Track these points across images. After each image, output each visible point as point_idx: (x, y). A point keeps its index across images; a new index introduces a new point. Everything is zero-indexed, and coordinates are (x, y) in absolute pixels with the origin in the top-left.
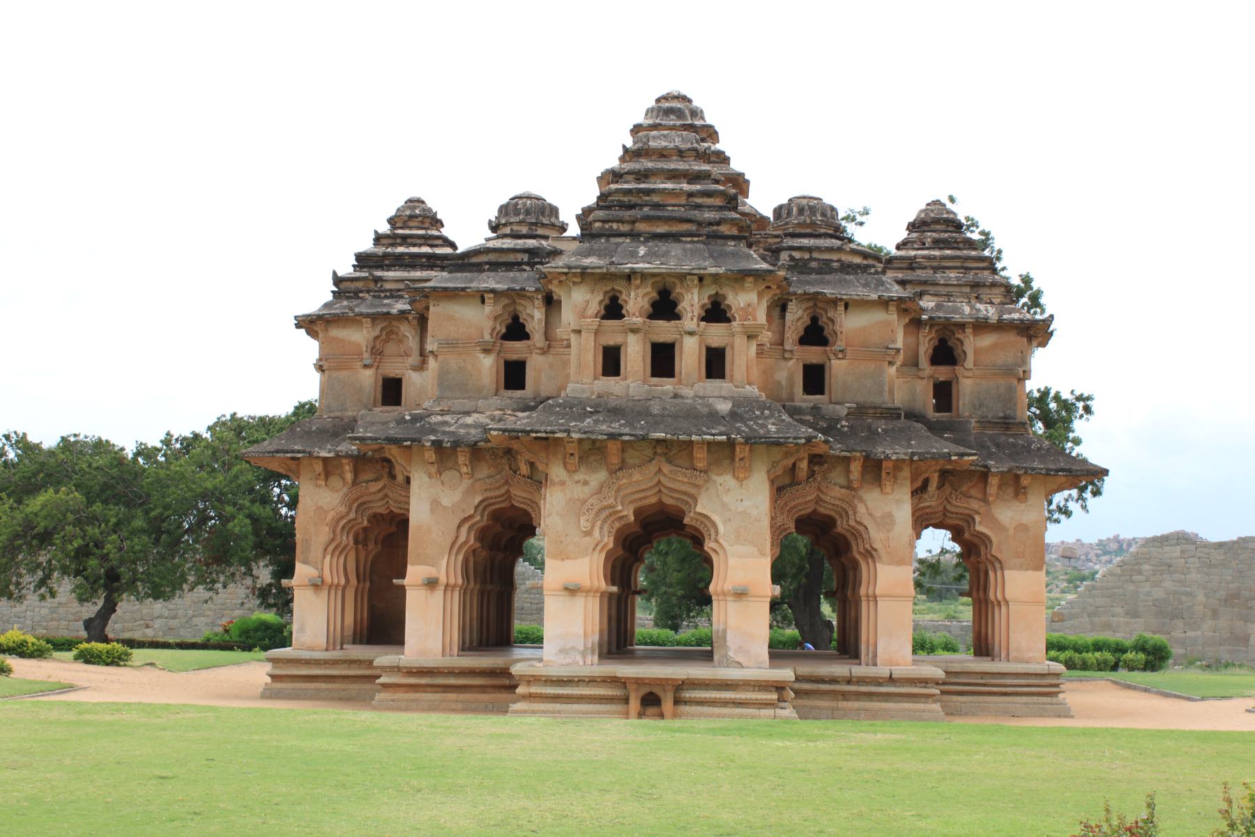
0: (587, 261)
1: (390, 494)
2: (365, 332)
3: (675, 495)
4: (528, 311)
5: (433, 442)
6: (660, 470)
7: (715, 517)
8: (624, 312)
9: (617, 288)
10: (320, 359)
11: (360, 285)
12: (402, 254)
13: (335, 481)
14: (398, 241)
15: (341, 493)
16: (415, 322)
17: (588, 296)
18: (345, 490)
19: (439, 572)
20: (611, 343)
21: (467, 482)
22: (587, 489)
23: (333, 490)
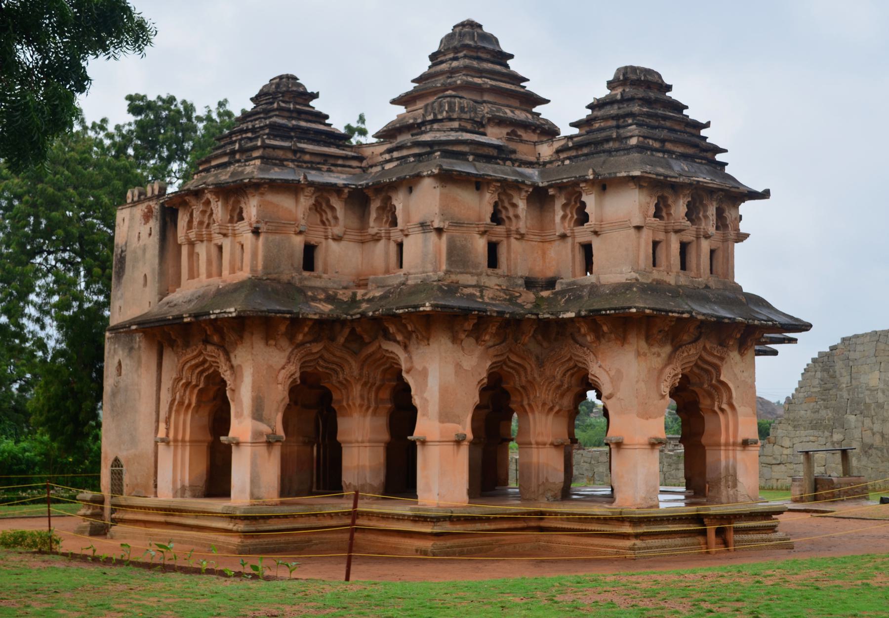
0: (661, 170)
1: (326, 355)
2: (302, 199)
3: (705, 366)
4: (515, 201)
5: (498, 312)
6: (705, 348)
7: (731, 385)
8: (664, 214)
9: (666, 194)
10: (257, 222)
11: (280, 153)
12: (309, 129)
13: (284, 343)
14: (294, 115)
15: (287, 353)
16: (345, 196)
17: (648, 199)
18: (290, 349)
19: (464, 429)
20: (657, 239)
21: (479, 350)
22: (659, 359)
23: (282, 349)
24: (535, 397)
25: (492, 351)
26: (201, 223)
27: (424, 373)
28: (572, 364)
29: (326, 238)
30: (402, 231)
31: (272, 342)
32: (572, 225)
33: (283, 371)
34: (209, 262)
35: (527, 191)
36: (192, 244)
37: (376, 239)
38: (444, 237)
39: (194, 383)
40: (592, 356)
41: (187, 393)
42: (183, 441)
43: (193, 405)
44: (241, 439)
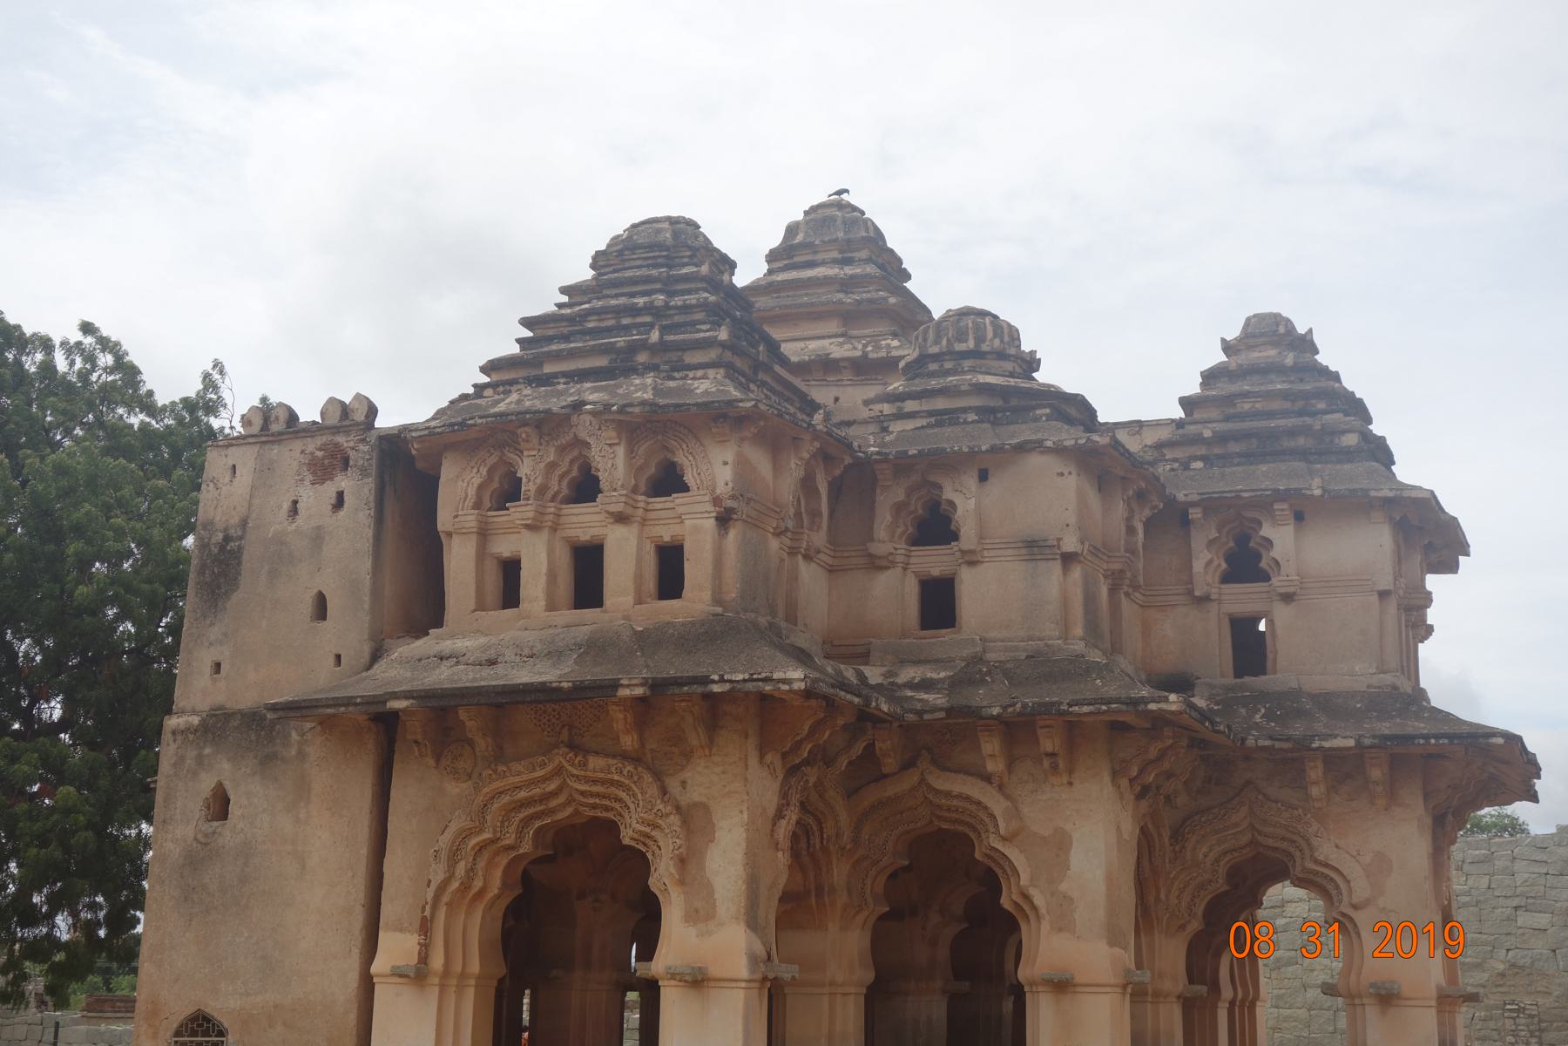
10: (733, 497)
16: (837, 472)
24: (1158, 899)
25: (1144, 804)
26: (542, 490)
27: (1061, 844)
28: (1244, 839)
29: (793, 552)
30: (963, 552)
31: (769, 758)
32: (1217, 579)
33: (783, 822)
34: (552, 575)
35: (1154, 507)
36: (484, 534)
37: (875, 565)
38: (1077, 573)
39: (507, 842)
40: (1315, 826)
41: (481, 864)
42: (463, 975)
43: (494, 890)
44: (714, 971)
